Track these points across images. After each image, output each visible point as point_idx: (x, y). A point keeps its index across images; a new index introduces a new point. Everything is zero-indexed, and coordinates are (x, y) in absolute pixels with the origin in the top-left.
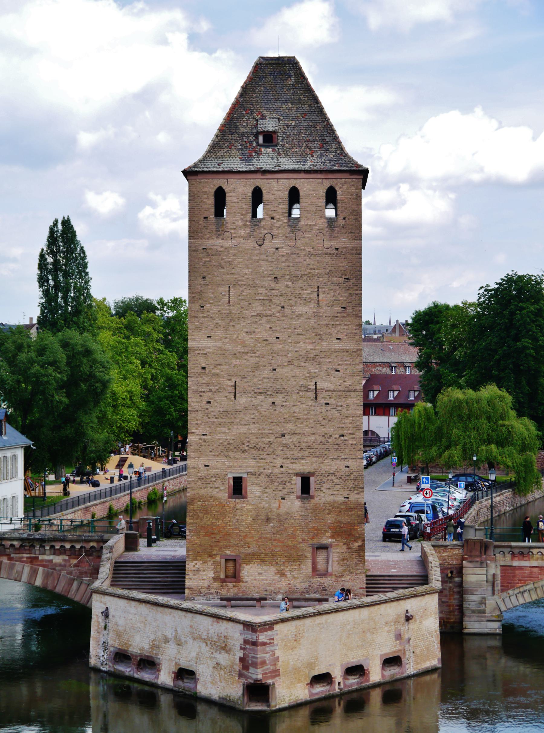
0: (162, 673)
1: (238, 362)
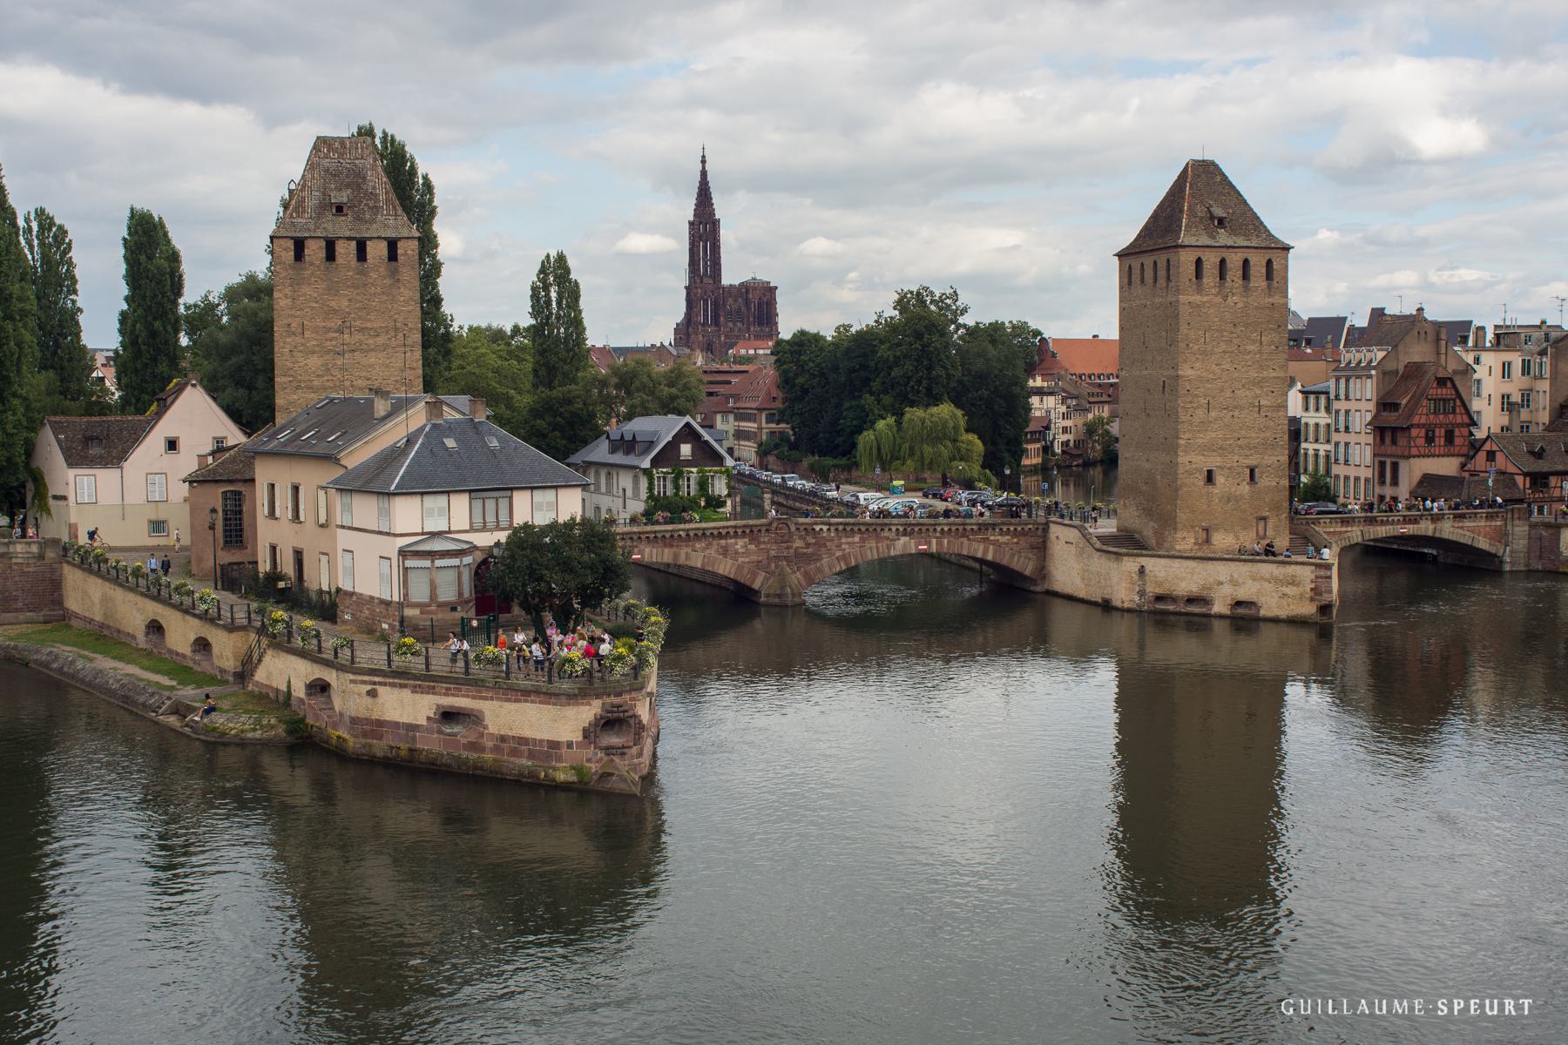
1: (1210, 386)
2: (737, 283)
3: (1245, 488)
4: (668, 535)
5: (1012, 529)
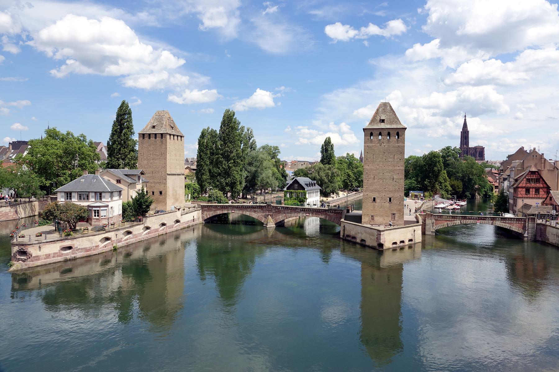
0: (357, 240)
2: (473, 146)
3: (387, 204)
4: (241, 207)
5: (334, 211)
